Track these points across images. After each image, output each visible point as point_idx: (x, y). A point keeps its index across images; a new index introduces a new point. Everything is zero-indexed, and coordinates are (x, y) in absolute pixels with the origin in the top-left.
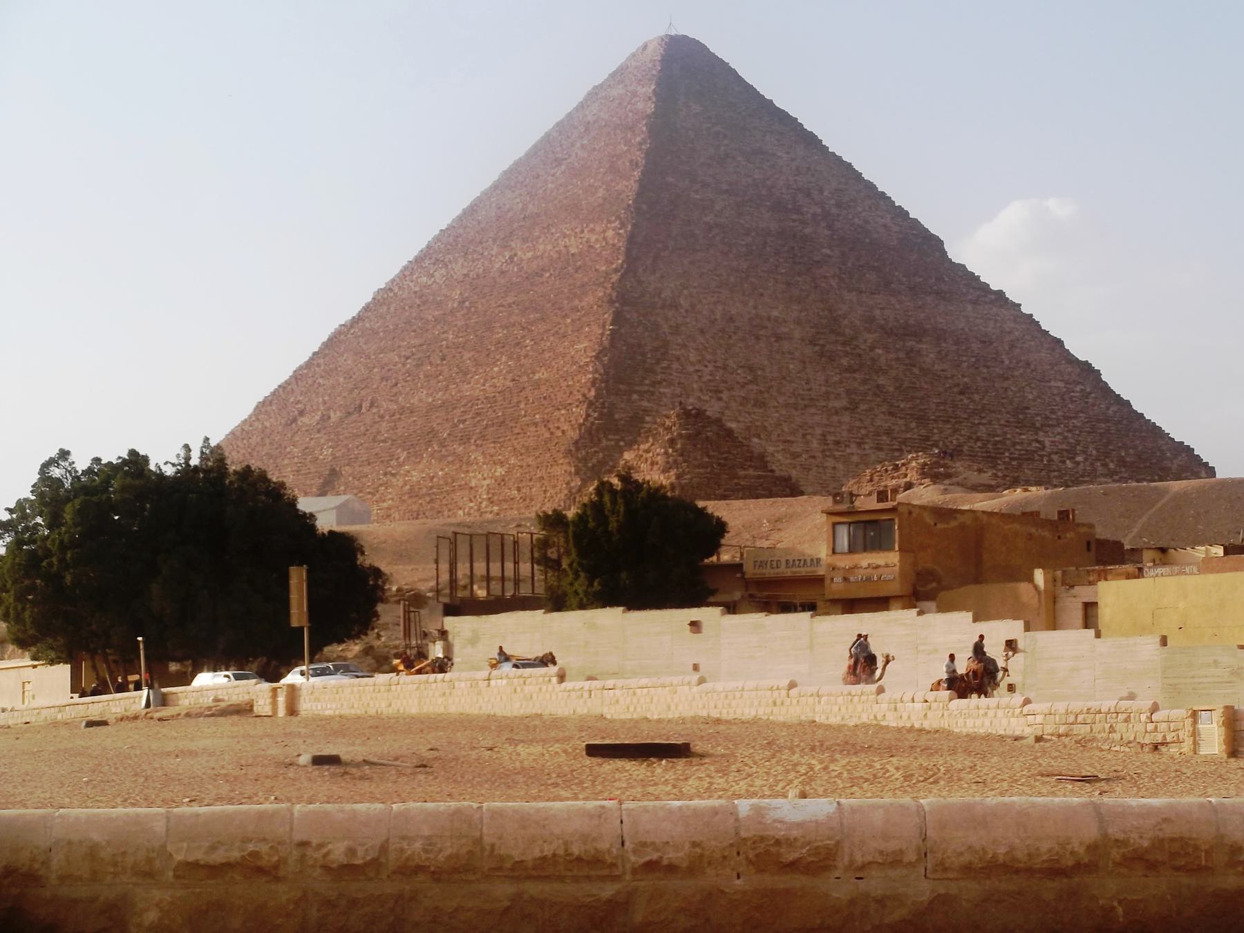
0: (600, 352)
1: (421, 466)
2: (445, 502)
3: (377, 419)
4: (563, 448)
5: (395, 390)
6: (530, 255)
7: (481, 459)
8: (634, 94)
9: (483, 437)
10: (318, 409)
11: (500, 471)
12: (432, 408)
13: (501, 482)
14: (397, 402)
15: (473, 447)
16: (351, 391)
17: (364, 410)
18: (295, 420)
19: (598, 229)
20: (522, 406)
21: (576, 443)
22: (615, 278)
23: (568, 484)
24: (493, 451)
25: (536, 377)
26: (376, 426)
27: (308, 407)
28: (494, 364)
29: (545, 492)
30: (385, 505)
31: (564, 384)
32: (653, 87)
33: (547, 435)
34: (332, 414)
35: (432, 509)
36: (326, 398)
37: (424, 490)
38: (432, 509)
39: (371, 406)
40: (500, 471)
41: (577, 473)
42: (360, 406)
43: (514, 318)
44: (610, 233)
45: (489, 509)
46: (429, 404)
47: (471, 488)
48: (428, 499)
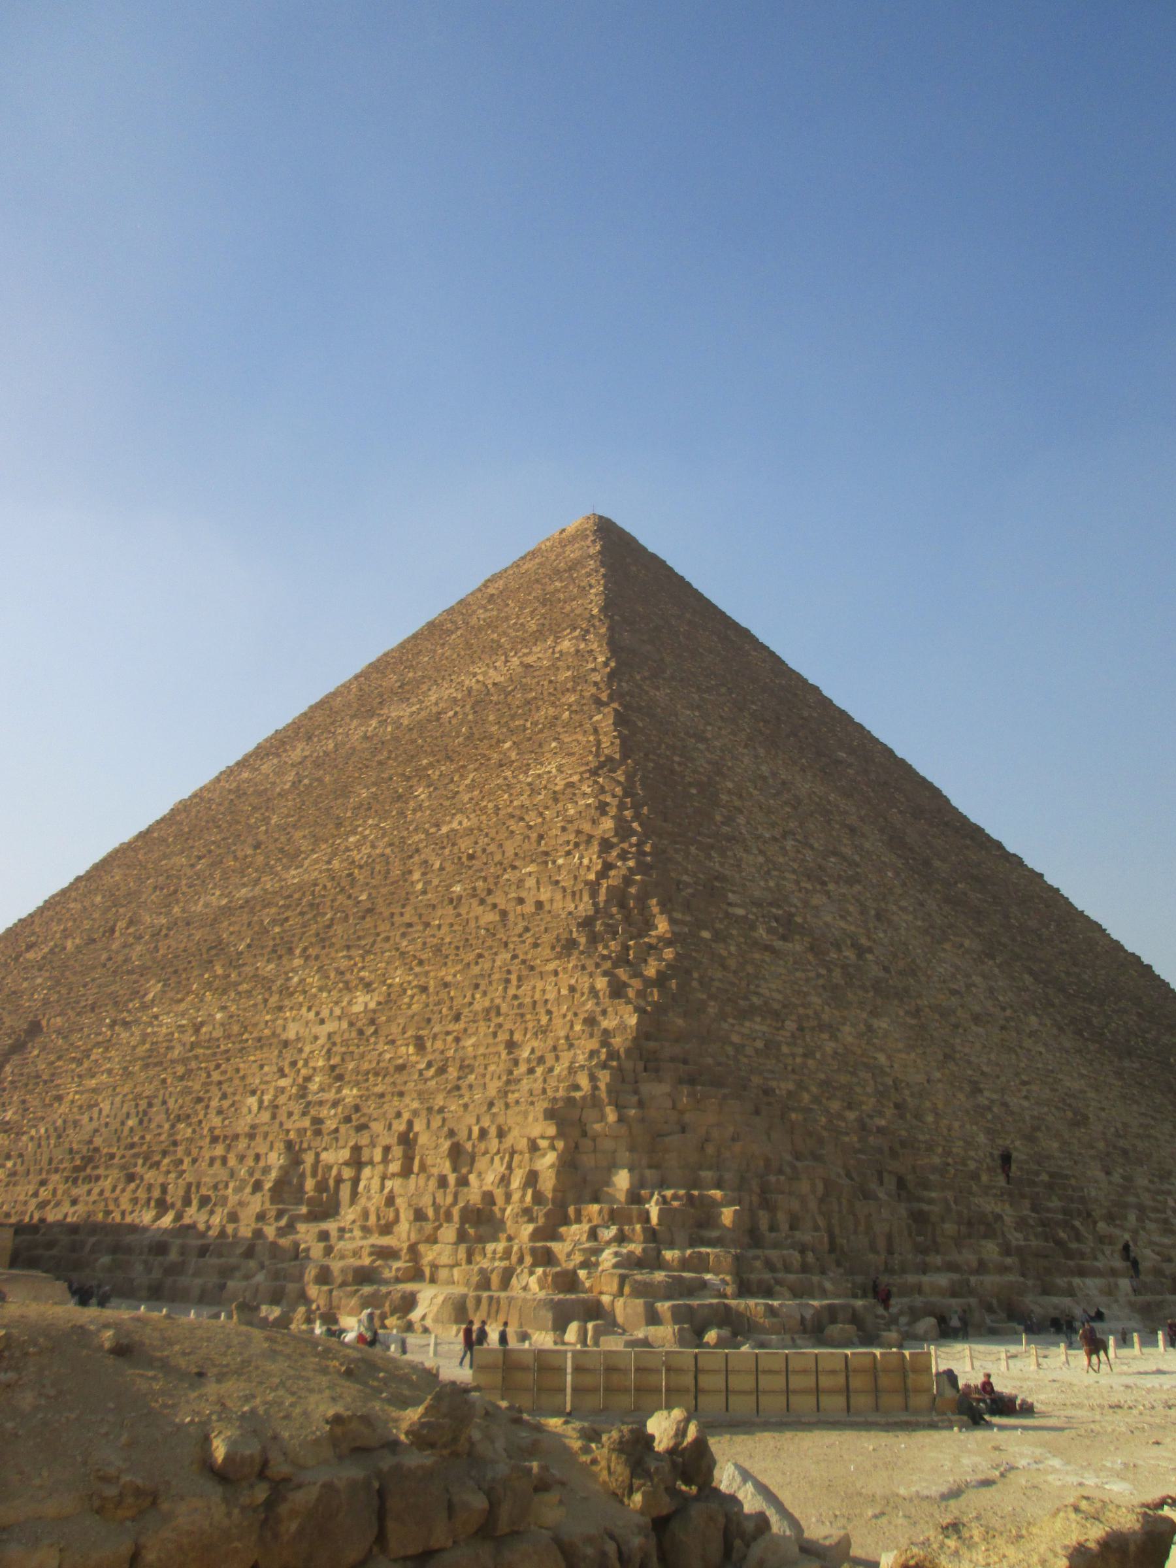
1: (183, 1006)
2: (216, 1076)
4: (546, 938)
7: (314, 980)
9: (323, 941)
11: (362, 1002)
13: (367, 1028)
14: (168, 914)
15: (297, 962)
20: (416, 876)
21: (587, 923)
23: (591, 1021)
24: (344, 964)
25: (445, 829)
26: (127, 951)
29: (511, 1045)
30: (93, 1082)
33: (492, 917)
35: (187, 1091)
37: (175, 1054)
38: (187, 1091)
40: (362, 1002)
41: (617, 990)
42: (113, 931)
45: (331, 1095)
47: (286, 1044)
48: (180, 1070)
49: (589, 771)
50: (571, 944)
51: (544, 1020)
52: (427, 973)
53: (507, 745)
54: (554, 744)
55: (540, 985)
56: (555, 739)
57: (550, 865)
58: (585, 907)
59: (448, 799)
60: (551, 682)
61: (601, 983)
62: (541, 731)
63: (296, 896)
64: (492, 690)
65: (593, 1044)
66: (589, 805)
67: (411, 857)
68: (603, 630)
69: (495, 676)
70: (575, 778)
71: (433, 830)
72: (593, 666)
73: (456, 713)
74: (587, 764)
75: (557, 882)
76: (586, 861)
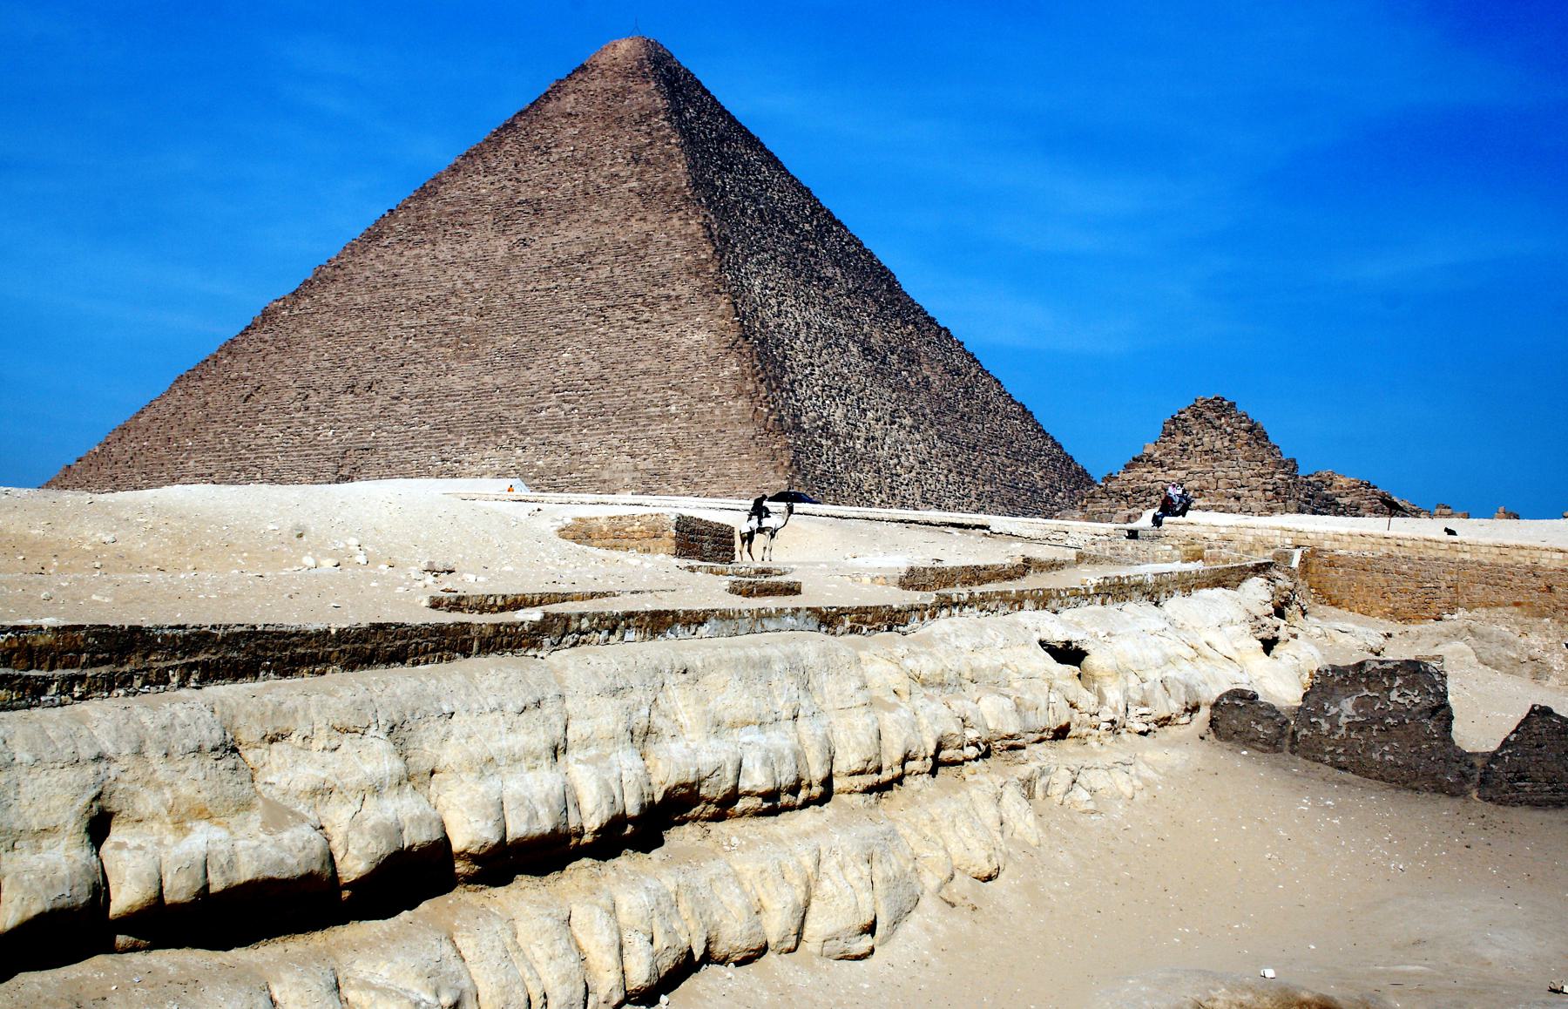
17: (357, 391)
19: (651, 217)
32: (653, 84)
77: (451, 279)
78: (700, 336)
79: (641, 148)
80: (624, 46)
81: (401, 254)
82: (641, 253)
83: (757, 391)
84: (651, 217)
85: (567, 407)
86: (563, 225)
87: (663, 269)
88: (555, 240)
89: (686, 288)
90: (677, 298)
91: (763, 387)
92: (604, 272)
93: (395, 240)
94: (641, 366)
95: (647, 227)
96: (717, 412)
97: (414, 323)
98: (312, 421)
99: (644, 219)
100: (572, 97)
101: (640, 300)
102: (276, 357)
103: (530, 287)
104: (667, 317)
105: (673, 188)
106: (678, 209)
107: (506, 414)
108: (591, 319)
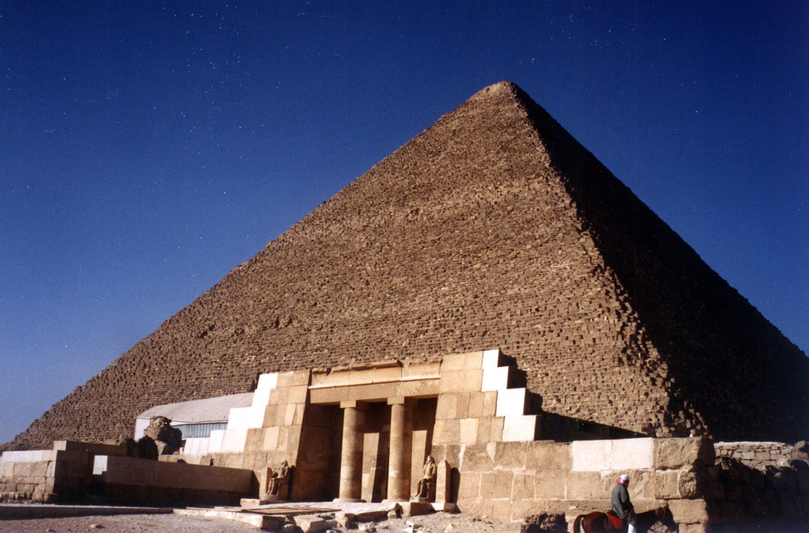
0: (596, 269)
3: (302, 332)
5: (315, 309)
6: (439, 207)
8: (498, 111)
10: (231, 325)
12: (368, 324)
14: (322, 318)
16: (264, 311)
17: (281, 325)
18: (205, 333)
22: (573, 212)
26: (304, 337)
27: (219, 324)
28: (443, 284)
31: (561, 298)
32: (516, 105)
34: (247, 329)
36: (238, 316)
39: (290, 322)
41: (653, 381)
42: (277, 323)
43: (445, 251)
44: (536, 186)
46: (366, 319)
49: (591, 272)
50: (620, 360)
51: (622, 393)
52: (545, 367)
53: (529, 247)
54: (560, 252)
55: (614, 378)
56: (560, 249)
57: (591, 320)
58: (620, 344)
59: (503, 274)
60: (538, 210)
61: (647, 379)
62: (547, 242)
63: (424, 318)
64: (496, 206)
65: (653, 403)
66: (600, 291)
67: (496, 305)
68: (558, 180)
69: (492, 198)
70: (586, 275)
71: (503, 291)
72: (563, 205)
73: (476, 218)
74: (589, 268)
75: (600, 330)
76: (611, 321)
77: (360, 242)
78: (566, 264)
79: (510, 142)
80: (495, 88)
81: (327, 229)
82: (509, 208)
83: (625, 309)
84: (516, 183)
85: (443, 330)
86: (446, 197)
87: (529, 217)
88: (439, 207)
89: (548, 230)
90: (541, 236)
91: (627, 304)
92: (479, 224)
93: (323, 219)
94: (510, 292)
95: (516, 191)
96: (584, 328)
97: (330, 273)
98: (242, 349)
99: (511, 186)
100: (457, 121)
101: (508, 242)
102: (228, 304)
103: (418, 241)
104: (533, 252)
105: (535, 162)
106: (538, 175)
107: (391, 338)
108: (467, 259)
